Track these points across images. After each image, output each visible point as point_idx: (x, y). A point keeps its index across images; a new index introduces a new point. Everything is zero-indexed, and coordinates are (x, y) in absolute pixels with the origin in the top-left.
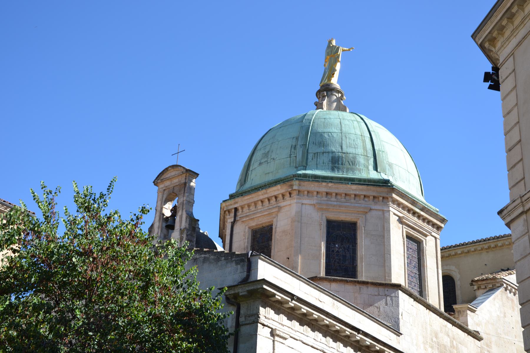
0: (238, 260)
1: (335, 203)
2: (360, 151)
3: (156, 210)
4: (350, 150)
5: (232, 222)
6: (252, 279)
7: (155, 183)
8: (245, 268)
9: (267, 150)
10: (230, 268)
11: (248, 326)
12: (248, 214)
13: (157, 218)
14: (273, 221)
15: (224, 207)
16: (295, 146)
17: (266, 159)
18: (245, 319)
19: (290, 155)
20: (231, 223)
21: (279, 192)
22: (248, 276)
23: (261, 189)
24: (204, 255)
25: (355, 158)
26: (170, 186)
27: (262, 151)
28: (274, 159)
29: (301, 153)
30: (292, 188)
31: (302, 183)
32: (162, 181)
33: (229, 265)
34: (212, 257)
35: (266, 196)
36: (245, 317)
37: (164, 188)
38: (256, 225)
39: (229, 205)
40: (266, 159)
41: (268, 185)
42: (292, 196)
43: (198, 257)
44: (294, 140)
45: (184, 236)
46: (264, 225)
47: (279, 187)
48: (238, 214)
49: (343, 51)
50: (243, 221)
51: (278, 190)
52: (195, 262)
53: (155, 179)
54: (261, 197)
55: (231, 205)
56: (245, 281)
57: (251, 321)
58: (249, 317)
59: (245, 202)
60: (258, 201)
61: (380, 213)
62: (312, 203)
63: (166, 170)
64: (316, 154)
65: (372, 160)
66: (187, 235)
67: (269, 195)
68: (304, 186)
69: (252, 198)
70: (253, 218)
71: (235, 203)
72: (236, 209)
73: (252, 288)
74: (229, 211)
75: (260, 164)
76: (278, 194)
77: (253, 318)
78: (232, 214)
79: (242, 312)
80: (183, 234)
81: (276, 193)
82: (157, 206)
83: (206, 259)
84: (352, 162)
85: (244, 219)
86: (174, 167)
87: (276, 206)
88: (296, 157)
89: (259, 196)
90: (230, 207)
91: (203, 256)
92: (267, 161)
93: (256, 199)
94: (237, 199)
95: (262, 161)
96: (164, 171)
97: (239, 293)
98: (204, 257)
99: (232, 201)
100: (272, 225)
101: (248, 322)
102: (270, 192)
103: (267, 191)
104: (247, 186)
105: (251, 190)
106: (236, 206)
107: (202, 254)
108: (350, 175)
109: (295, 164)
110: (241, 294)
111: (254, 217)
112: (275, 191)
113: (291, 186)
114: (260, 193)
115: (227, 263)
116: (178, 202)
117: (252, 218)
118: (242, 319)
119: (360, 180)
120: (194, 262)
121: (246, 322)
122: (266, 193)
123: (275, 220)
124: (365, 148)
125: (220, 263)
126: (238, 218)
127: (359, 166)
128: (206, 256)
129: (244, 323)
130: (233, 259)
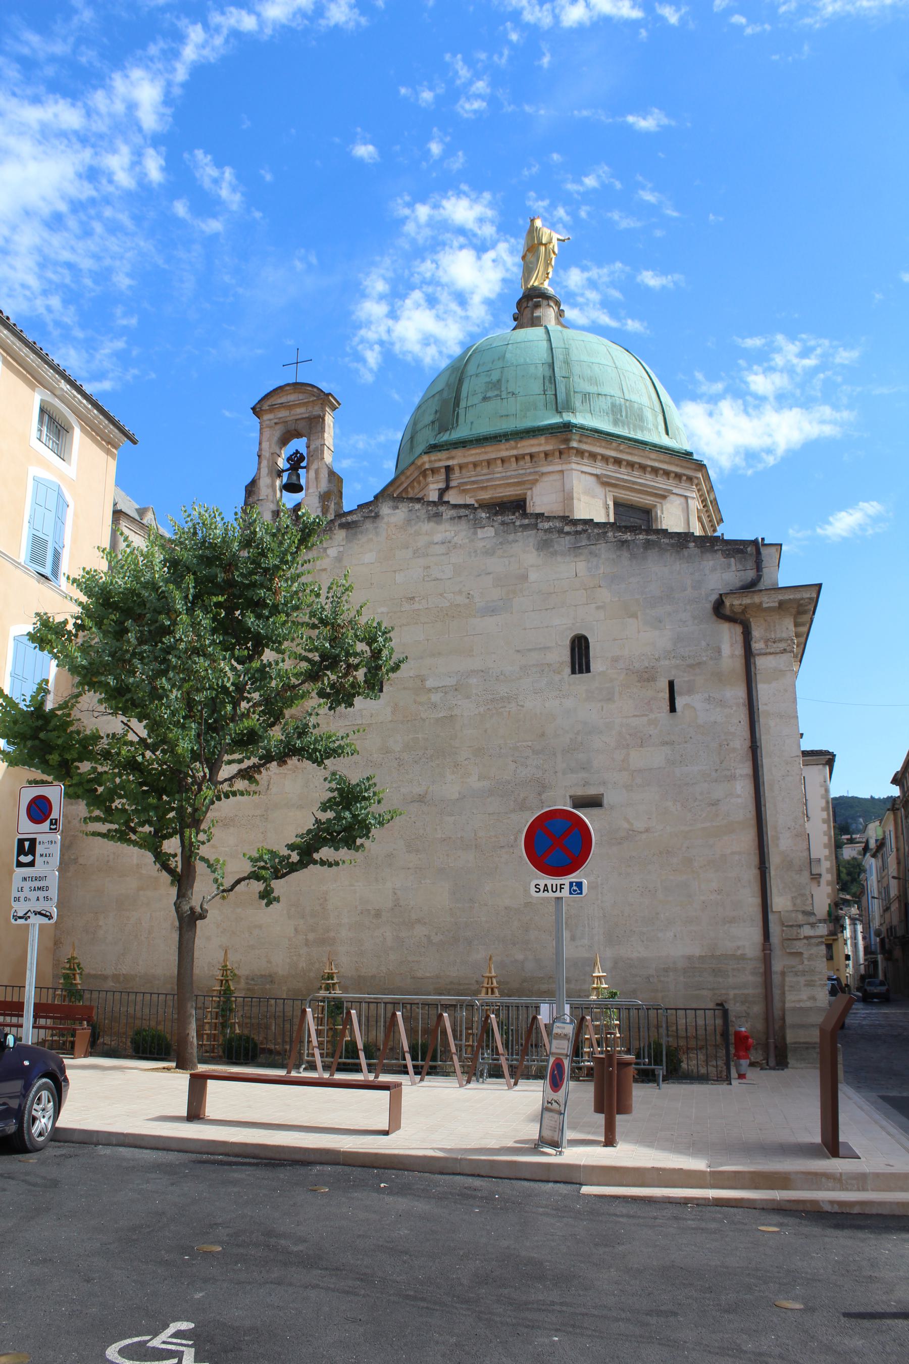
0: (727, 550)
1: (625, 477)
2: (645, 401)
3: (259, 456)
4: (634, 397)
5: (439, 489)
6: (765, 583)
7: (257, 411)
8: (750, 564)
9: (495, 376)
10: (711, 563)
11: (770, 657)
12: (473, 479)
13: (264, 471)
14: (525, 494)
15: (424, 463)
16: (550, 377)
17: (496, 393)
18: (767, 646)
19: (544, 391)
20: (437, 491)
21: (542, 449)
22: (759, 578)
23: (503, 441)
24: (645, 537)
25: (641, 409)
26: (289, 419)
27: (483, 379)
28: (513, 394)
29: (564, 390)
30: (568, 444)
31: (585, 440)
32: (272, 409)
33: (709, 555)
34: (666, 541)
35: (515, 452)
36: (767, 641)
37: (276, 421)
38: (491, 498)
39: (435, 461)
40: (496, 393)
41: (511, 434)
42: (562, 456)
43: (629, 538)
44: (546, 368)
45: (329, 504)
46: (505, 499)
47: (542, 439)
48: (452, 476)
49: (558, 240)
50: (464, 490)
51: (540, 445)
52: (625, 547)
53: (257, 404)
54: (504, 454)
55: (440, 460)
56: (750, 586)
57: (778, 650)
58: (774, 642)
59: (471, 459)
60: (495, 459)
61: (682, 500)
62: (595, 473)
63: (281, 388)
64: (586, 396)
65: (660, 418)
66: (335, 504)
67: (521, 452)
68: (586, 443)
69: (486, 453)
70: (487, 486)
71: (448, 459)
72: (448, 469)
73: (791, 597)
74: (434, 471)
75: (485, 399)
76: (539, 452)
77: (782, 645)
78: (442, 476)
79: (756, 633)
80: (328, 501)
81: (534, 450)
82: (260, 449)
83: (651, 543)
84: (638, 415)
85: (468, 487)
86: (297, 386)
87: (532, 470)
88: (556, 395)
89: (500, 450)
90: (437, 465)
91: (641, 537)
92: (500, 396)
93: (493, 456)
94: (454, 452)
95: (489, 394)
96: (275, 390)
97: (761, 603)
98: (646, 539)
99: (443, 455)
100: (524, 501)
101: (772, 650)
102: (523, 446)
103: (517, 443)
104: (461, 432)
105: (476, 440)
106: (450, 463)
107: (640, 534)
108: (639, 436)
109: (554, 407)
110: (765, 605)
111: (488, 484)
112: (532, 445)
113: (567, 441)
114: (503, 446)
115: (702, 552)
116: (308, 447)
117: (485, 485)
118: (757, 646)
119: (655, 446)
120: (623, 545)
121: (768, 651)
122: (516, 448)
123: (529, 493)
124: (650, 397)
125: (686, 552)
126: (453, 484)
127: (647, 424)
128: (649, 537)
129: (763, 651)
130: (716, 548)
